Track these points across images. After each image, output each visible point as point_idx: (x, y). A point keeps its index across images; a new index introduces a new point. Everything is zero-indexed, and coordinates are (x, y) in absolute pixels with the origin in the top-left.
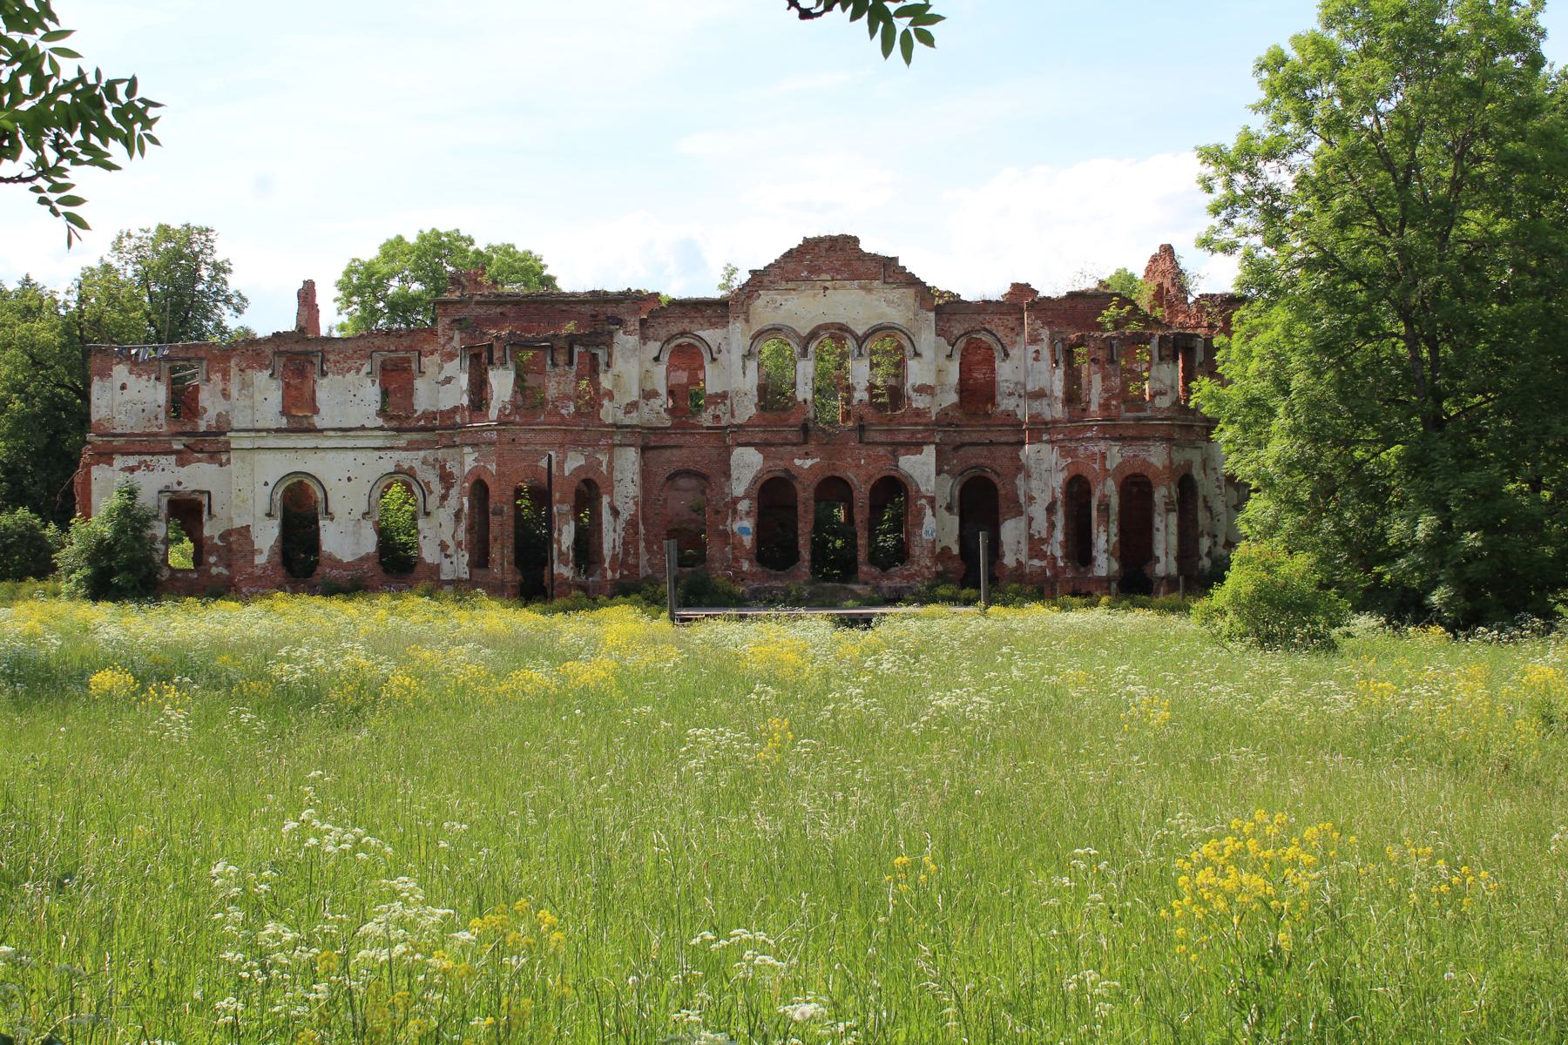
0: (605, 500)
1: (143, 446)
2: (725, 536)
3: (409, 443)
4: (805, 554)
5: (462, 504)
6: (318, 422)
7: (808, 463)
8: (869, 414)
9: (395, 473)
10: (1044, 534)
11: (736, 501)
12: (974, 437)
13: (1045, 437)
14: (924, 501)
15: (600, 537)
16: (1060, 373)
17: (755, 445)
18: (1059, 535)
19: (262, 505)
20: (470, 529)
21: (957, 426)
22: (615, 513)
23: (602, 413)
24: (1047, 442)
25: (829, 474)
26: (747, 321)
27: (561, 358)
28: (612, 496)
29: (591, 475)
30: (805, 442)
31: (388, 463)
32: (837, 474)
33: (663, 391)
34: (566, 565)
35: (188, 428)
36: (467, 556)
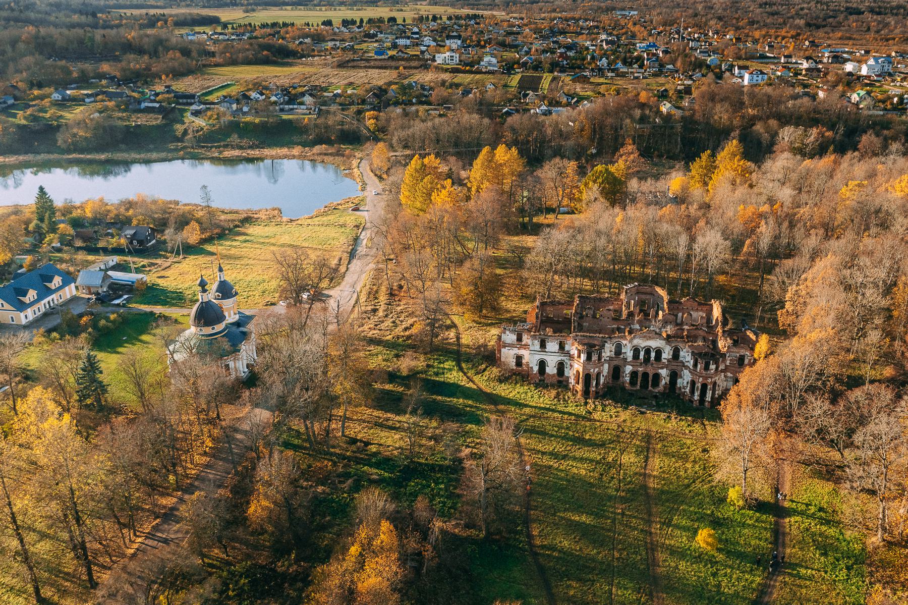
1: (511, 346)
6: (547, 350)
31: (560, 358)
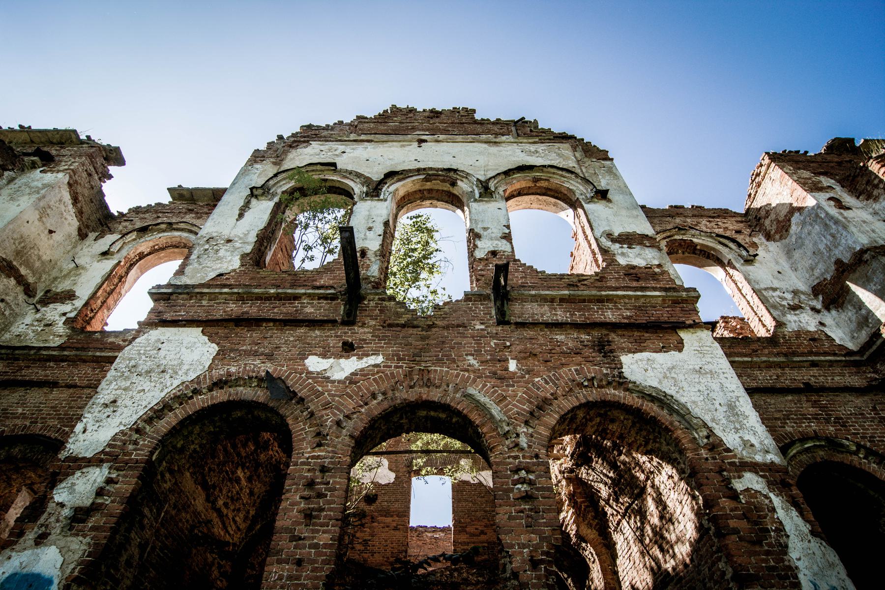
7: (348, 366)
25: (411, 396)
30: (349, 320)
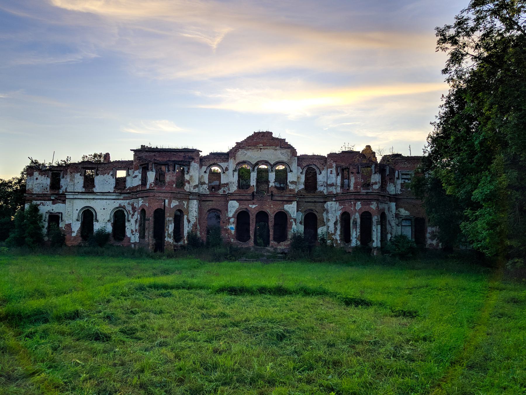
0: (185, 217)
1: (43, 197)
2: (227, 230)
3: (124, 197)
4: (252, 237)
5: (138, 217)
6: (95, 190)
7: (254, 206)
8: (275, 191)
9: (119, 207)
10: (333, 232)
11: (229, 218)
12: (309, 200)
13: (334, 199)
14: (292, 220)
15: (183, 229)
16: (339, 178)
17: (237, 200)
18: (338, 232)
19: (75, 217)
20: (140, 226)
21: (304, 196)
22: (189, 221)
23: (185, 187)
24: (334, 201)
25: (261, 210)
26: (235, 159)
27: (171, 169)
28: (188, 216)
29: (180, 208)
30: (253, 199)
31: (117, 204)
32: (263, 210)
33: (207, 182)
34: (170, 238)
35: (56, 192)
36: (139, 234)
